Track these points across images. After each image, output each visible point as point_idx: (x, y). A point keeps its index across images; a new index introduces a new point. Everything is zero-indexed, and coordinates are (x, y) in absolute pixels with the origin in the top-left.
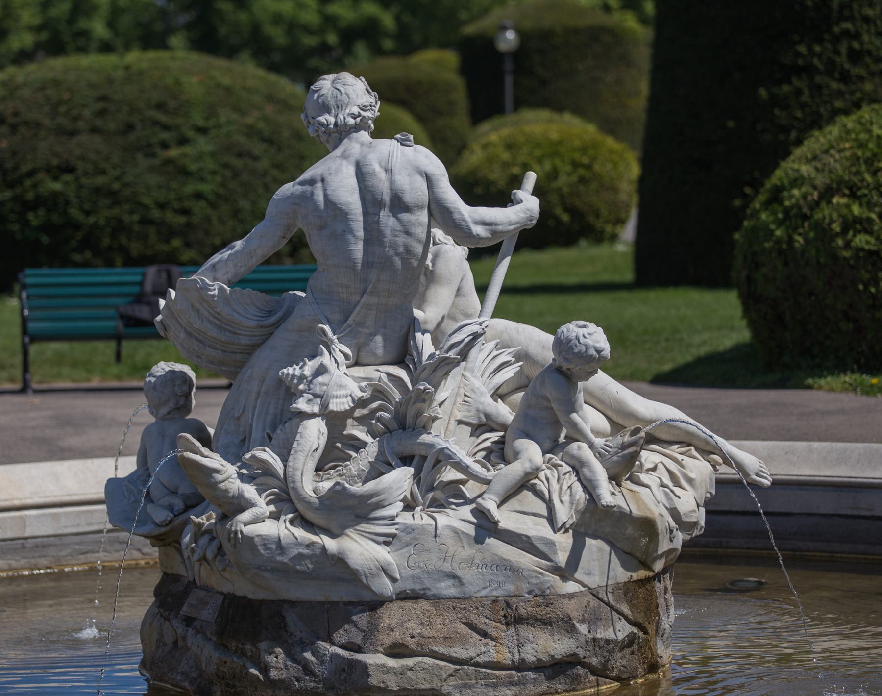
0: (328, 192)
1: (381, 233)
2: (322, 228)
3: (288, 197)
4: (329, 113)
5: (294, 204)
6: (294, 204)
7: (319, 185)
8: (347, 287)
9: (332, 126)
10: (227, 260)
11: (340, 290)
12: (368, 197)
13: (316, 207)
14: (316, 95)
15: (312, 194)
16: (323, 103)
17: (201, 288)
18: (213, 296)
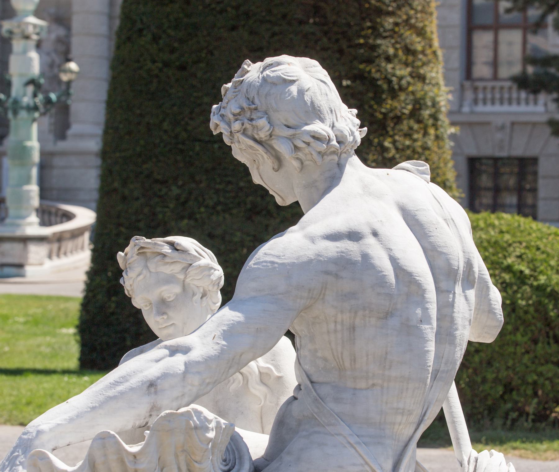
0: (398, 254)
1: (452, 320)
2: (388, 315)
3: (310, 261)
4: (322, 120)
5: (327, 273)
6: (327, 273)
7: (371, 240)
8: (410, 413)
9: (334, 142)
10: (185, 373)
11: (399, 418)
12: (440, 262)
13: (381, 280)
14: (294, 89)
15: (365, 257)
16: (312, 103)
17: (196, 428)
18: (210, 440)
